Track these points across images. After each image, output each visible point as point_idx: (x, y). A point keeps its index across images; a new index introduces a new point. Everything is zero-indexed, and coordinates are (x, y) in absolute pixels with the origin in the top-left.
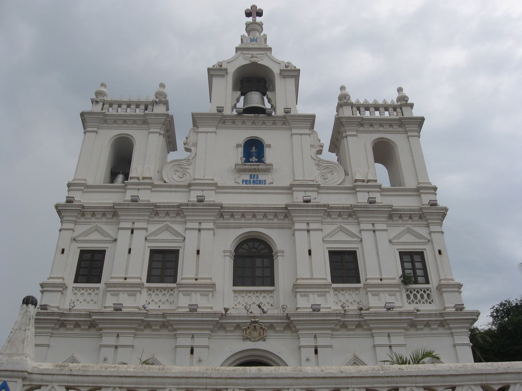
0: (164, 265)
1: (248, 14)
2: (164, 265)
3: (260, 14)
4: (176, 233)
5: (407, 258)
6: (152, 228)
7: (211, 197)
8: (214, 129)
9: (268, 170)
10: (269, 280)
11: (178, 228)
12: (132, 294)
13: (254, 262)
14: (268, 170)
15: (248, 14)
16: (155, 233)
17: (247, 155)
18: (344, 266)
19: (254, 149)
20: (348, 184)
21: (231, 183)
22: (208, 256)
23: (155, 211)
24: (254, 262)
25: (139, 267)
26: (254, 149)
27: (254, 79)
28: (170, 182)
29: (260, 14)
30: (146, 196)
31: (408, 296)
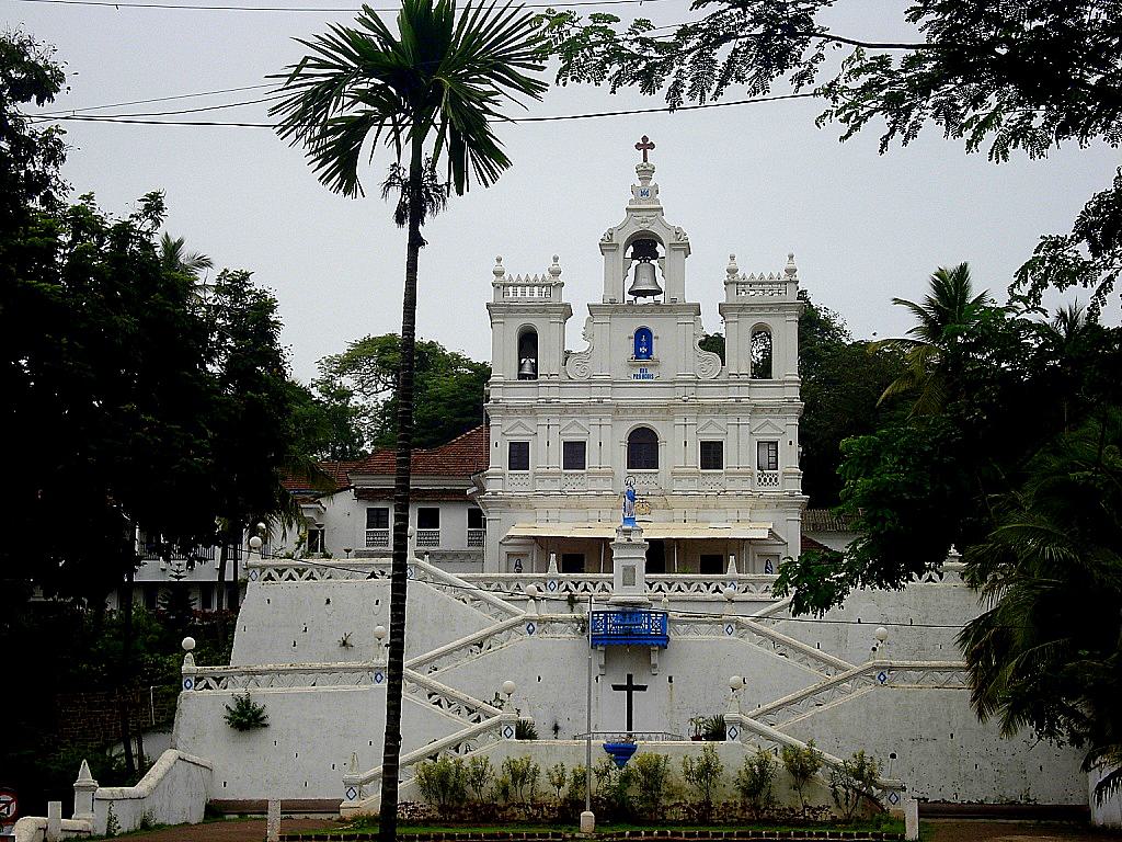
0: (574, 455)
1: (638, 146)
2: (574, 455)
3: (652, 146)
4: (582, 428)
5: (764, 451)
6: (565, 423)
7: (606, 394)
8: (607, 320)
9: (656, 364)
10: (653, 463)
11: (581, 422)
12: (554, 480)
13: (643, 449)
14: (656, 364)
15: (638, 146)
16: (567, 428)
17: (638, 344)
18: (712, 455)
19: (643, 338)
20: (722, 378)
21: (624, 377)
22: (608, 449)
23: (565, 409)
24: (643, 449)
25: (557, 456)
26: (643, 338)
27: (644, 246)
28: (576, 379)
29: (652, 146)
30: (553, 394)
31: (760, 479)
